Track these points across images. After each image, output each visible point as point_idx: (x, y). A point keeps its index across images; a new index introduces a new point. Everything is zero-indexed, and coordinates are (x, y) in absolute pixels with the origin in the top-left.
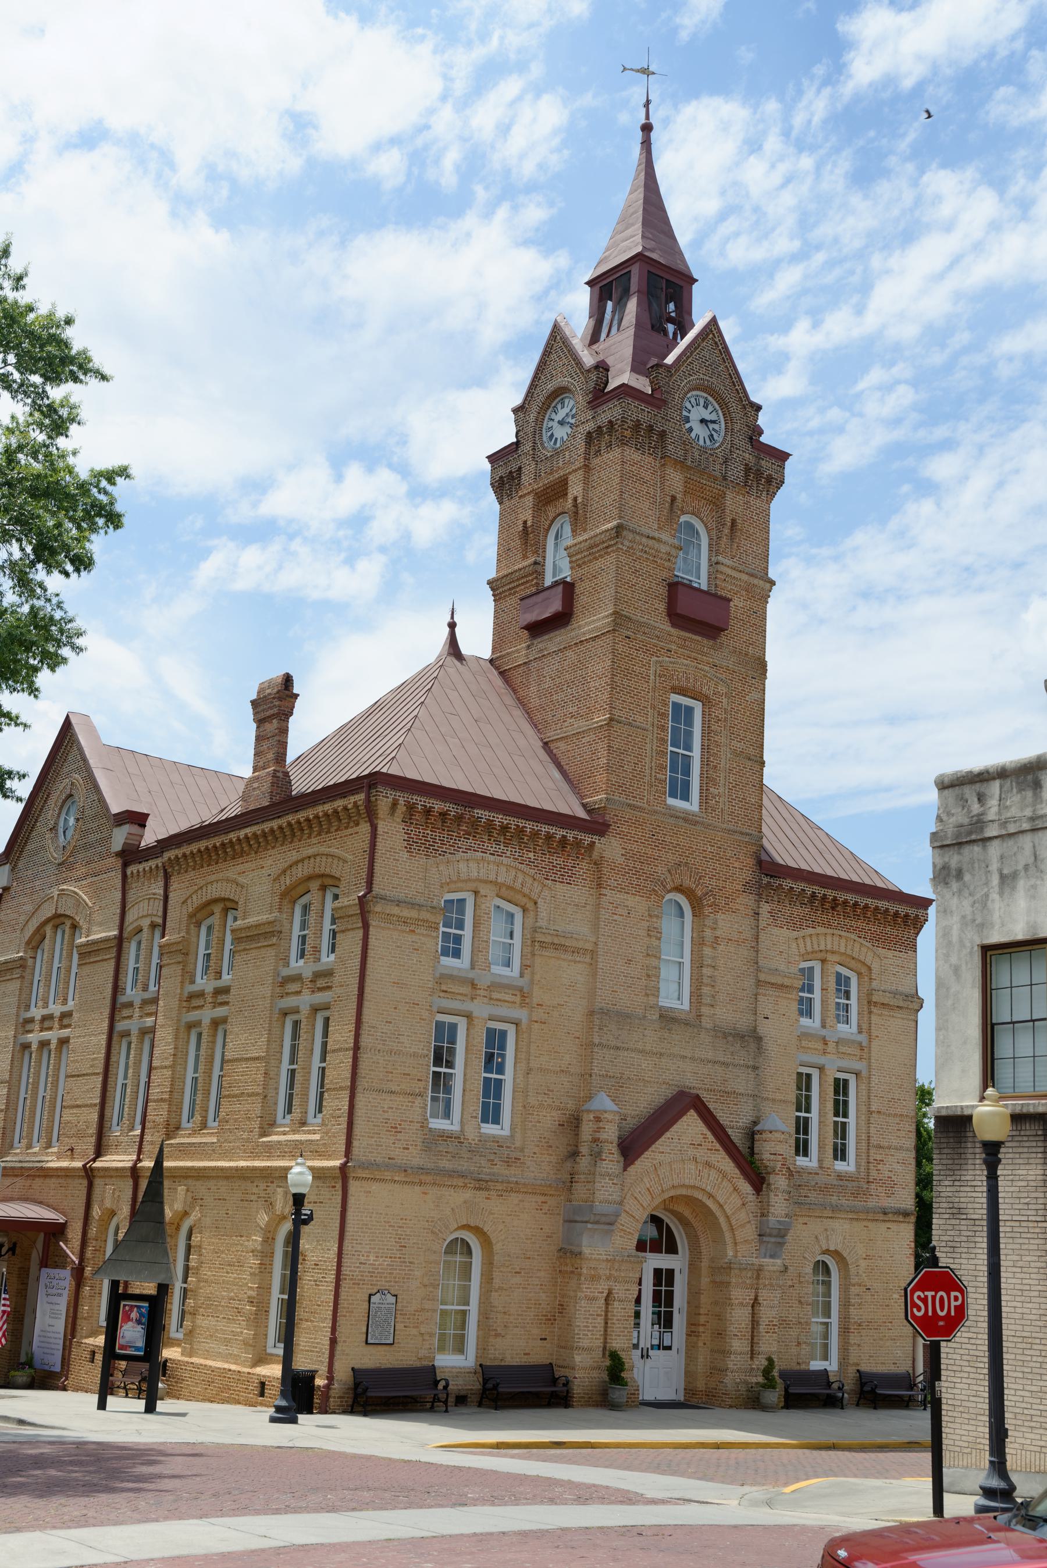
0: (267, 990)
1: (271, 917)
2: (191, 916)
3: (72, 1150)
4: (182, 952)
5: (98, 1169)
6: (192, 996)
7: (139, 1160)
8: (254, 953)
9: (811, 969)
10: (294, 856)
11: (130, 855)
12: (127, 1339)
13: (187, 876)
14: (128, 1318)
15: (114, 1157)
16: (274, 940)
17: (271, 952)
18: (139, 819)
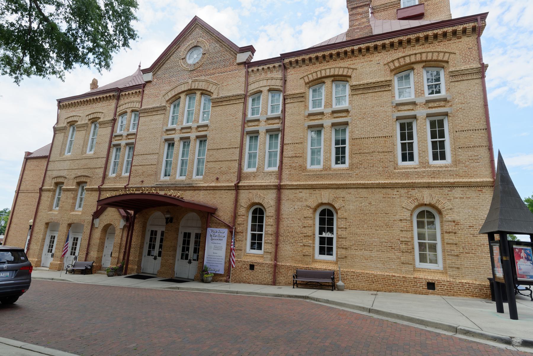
0: (390, 109)
1: (388, 79)
2: (306, 84)
3: (217, 179)
4: (301, 97)
5: (241, 186)
6: (310, 115)
7: (280, 182)
8: (370, 95)
9: (312, 164)
10: (401, 54)
11: (248, 64)
12: (523, 270)
13: (303, 68)
14: (520, 257)
15: (247, 182)
16: (390, 88)
17: (388, 93)
18: (251, 49)
